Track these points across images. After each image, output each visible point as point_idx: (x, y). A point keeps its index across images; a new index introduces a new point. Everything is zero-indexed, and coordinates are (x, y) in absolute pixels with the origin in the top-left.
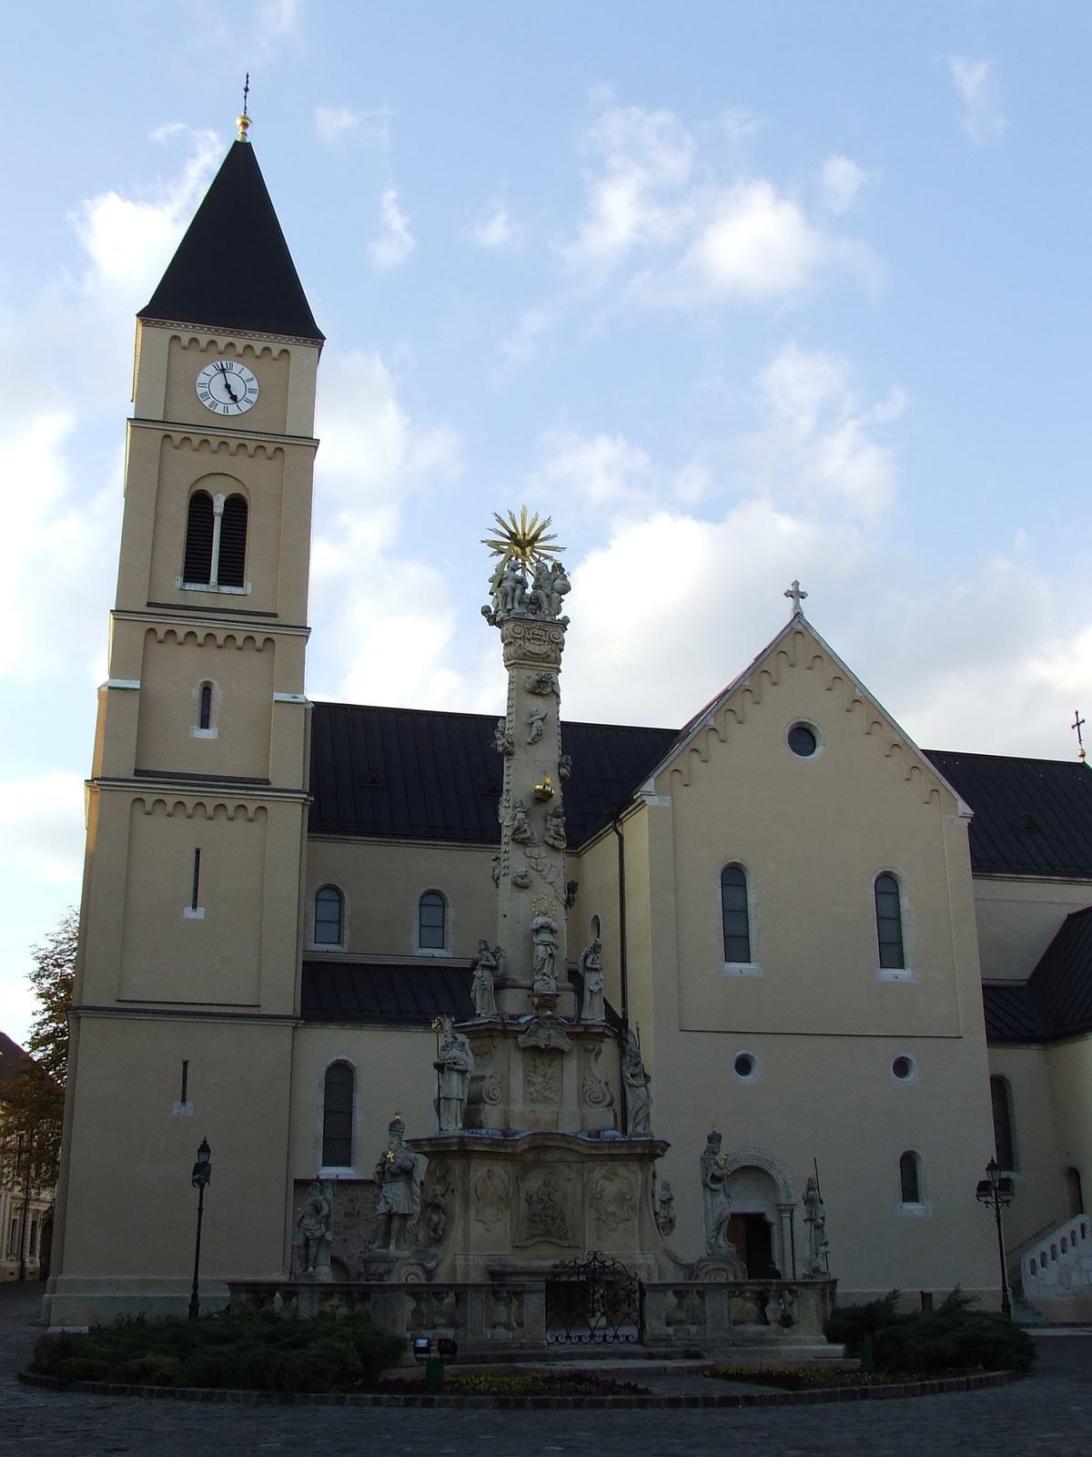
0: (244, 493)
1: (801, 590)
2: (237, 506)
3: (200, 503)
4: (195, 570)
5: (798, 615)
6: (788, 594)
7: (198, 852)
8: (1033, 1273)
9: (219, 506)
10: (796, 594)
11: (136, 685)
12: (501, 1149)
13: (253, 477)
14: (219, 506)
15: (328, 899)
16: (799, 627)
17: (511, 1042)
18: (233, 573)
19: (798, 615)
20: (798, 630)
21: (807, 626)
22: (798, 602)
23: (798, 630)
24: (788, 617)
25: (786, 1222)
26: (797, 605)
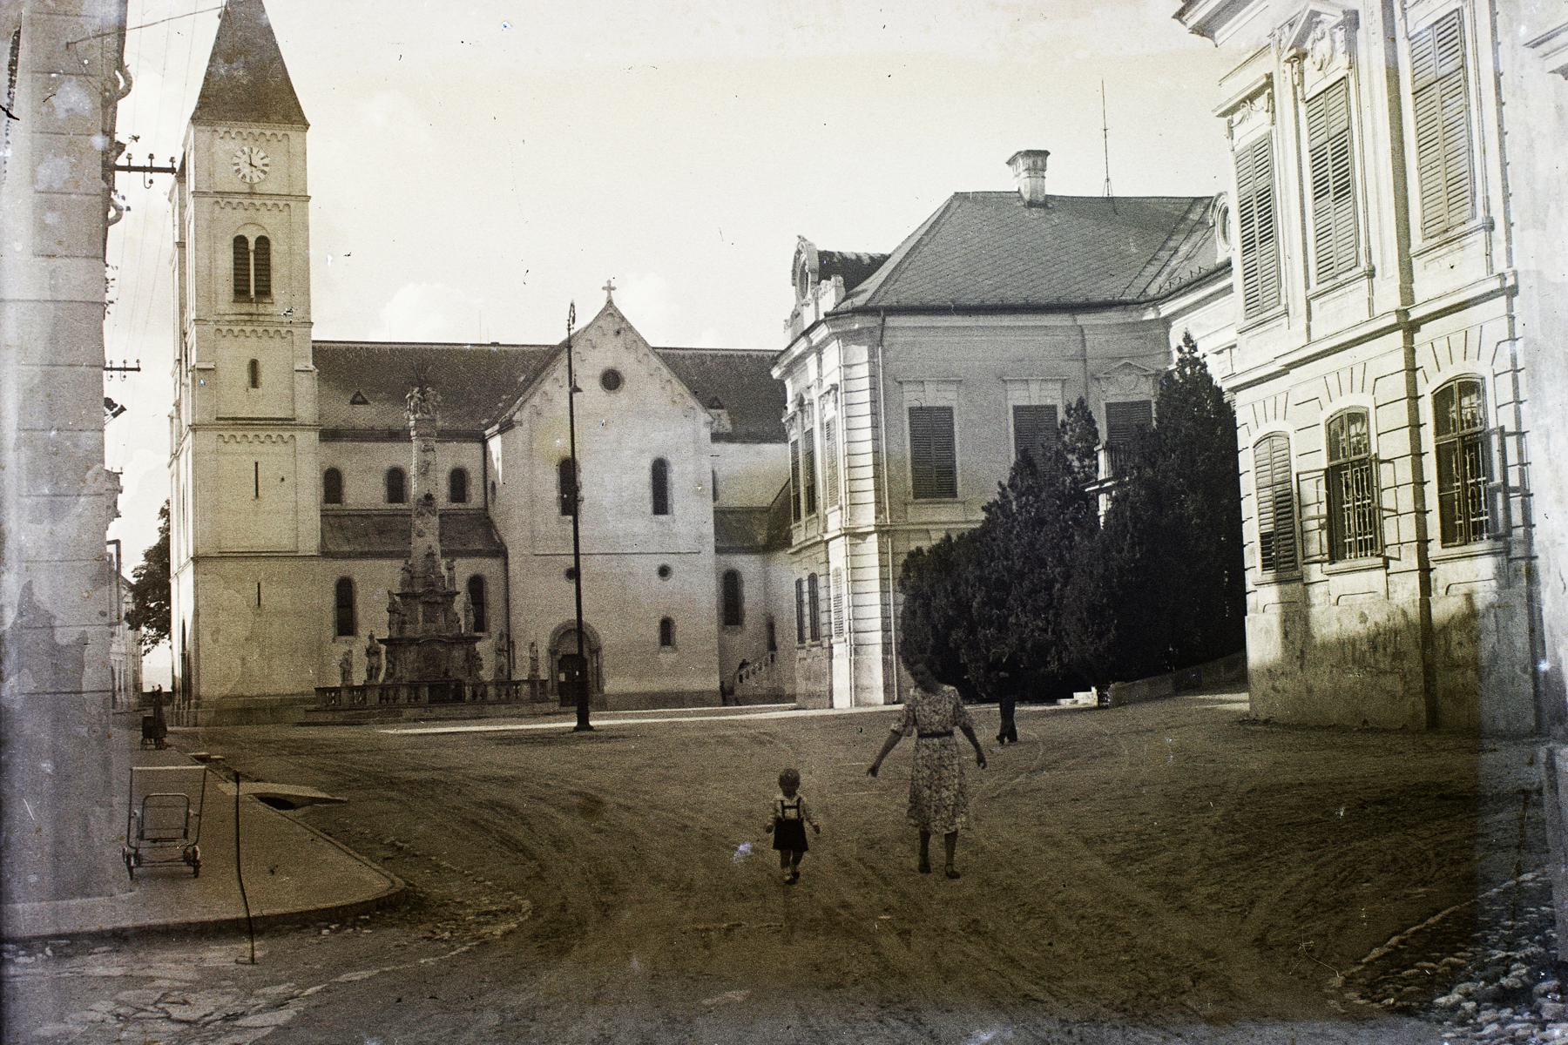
1: (612, 285)
2: (263, 242)
3: (240, 242)
4: (241, 293)
5: (610, 302)
8: (741, 681)
9: (252, 246)
12: (413, 641)
13: (270, 223)
14: (252, 246)
15: (333, 483)
18: (264, 291)
19: (610, 302)
21: (616, 310)
22: (610, 293)
24: (603, 304)
25: (595, 659)
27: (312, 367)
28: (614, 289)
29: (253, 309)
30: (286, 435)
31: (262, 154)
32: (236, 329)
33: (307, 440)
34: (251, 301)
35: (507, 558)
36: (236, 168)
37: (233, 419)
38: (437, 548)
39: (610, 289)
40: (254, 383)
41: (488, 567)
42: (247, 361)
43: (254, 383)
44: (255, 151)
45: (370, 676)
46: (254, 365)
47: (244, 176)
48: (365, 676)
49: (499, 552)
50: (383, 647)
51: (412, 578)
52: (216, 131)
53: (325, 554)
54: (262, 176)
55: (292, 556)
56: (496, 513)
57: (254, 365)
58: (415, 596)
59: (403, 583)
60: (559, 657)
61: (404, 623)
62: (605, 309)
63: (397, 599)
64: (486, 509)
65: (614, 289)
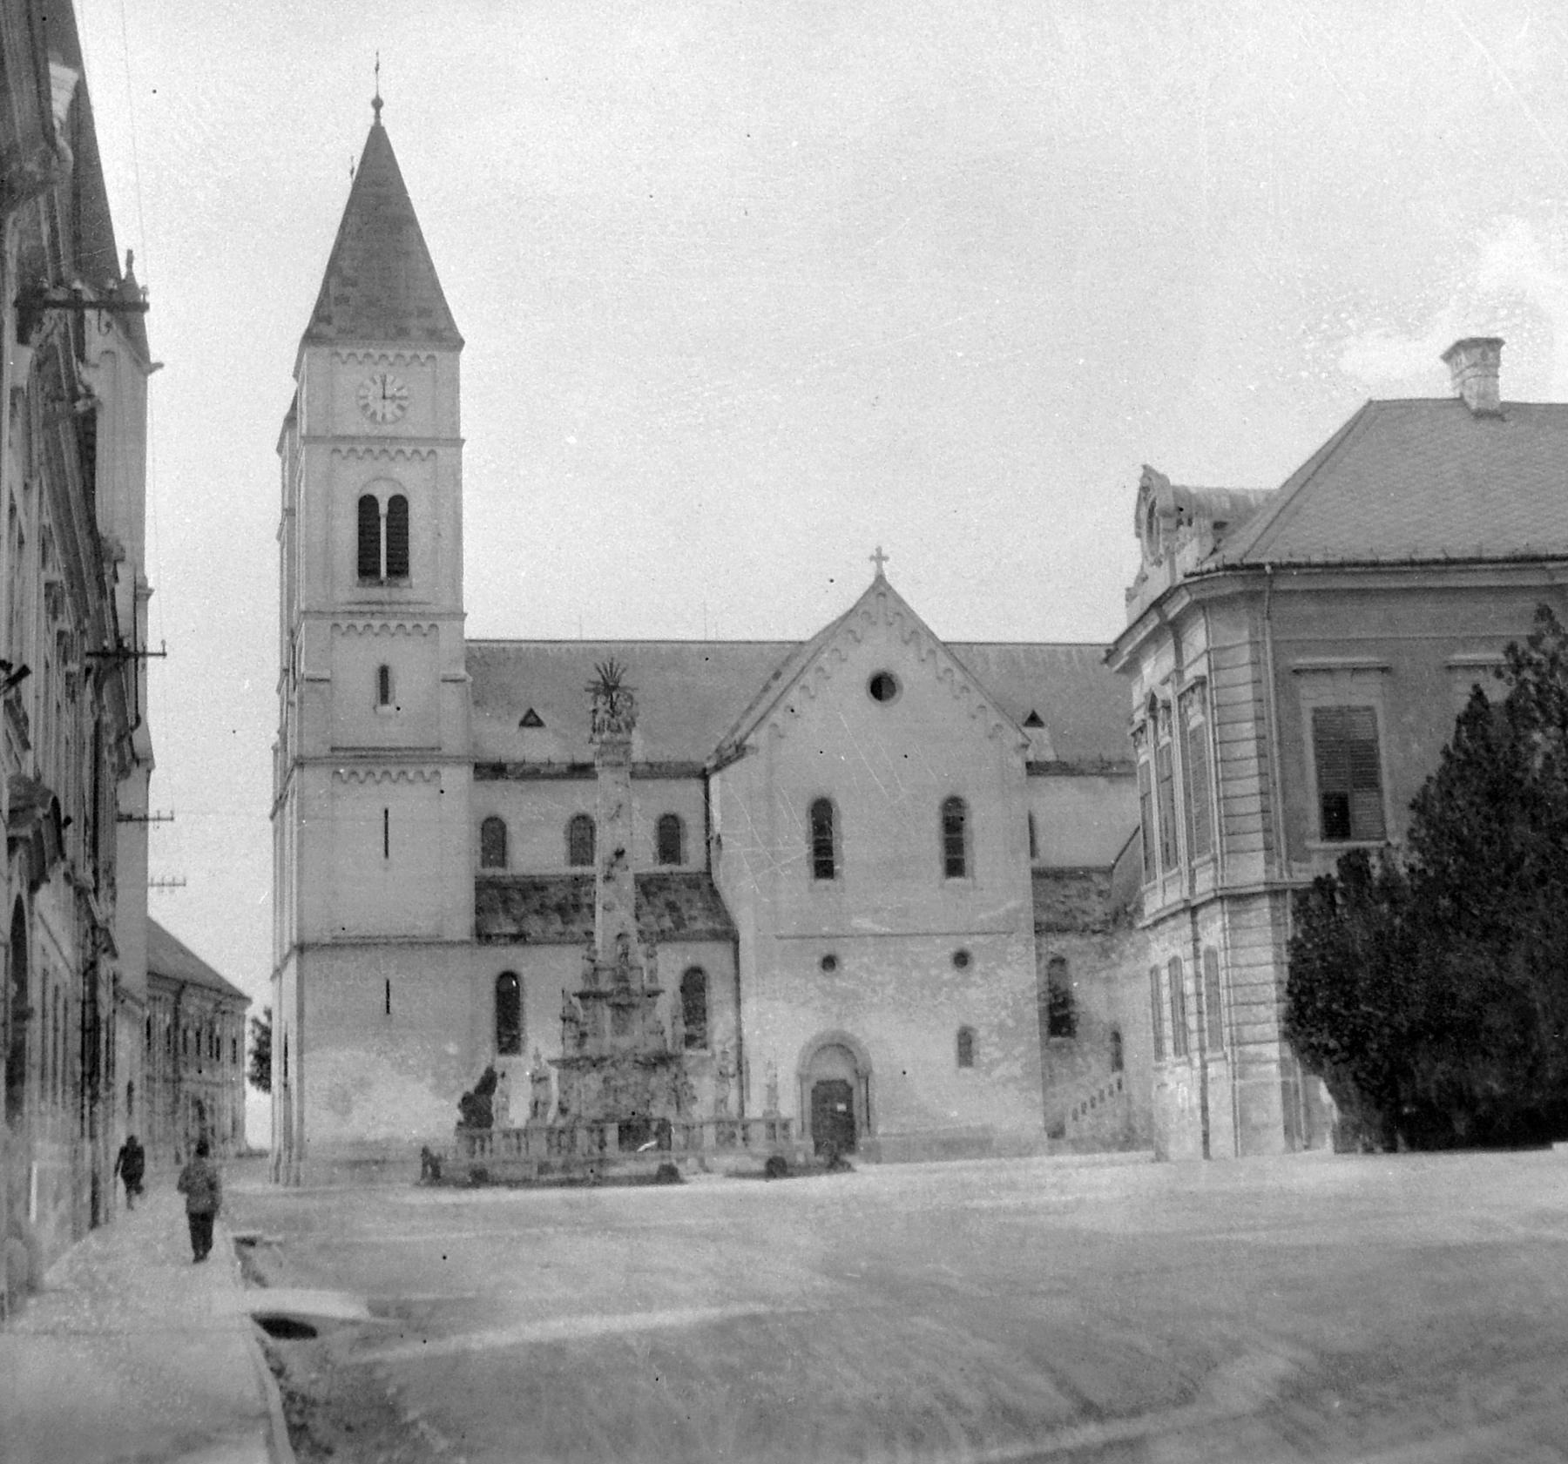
0: (401, 492)
2: (399, 505)
3: (367, 505)
4: (367, 569)
5: (880, 578)
6: (872, 558)
7: (386, 812)
9: (383, 509)
10: (879, 558)
11: (326, 674)
13: (409, 478)
14: (383, 509)
15: (494, 837)
16: (882, 589)
17: (604, 1001)
18: (399, 567)
19: (880, 578)
20: (880, 588)
22: (879, 566)
23: (880, 588)
26: (879, 566)
27: (462, 673)
28: (886, 559)
29: (377, 593)
30: (428, 770)
31: (399, 383)
32: (360, 623)
33: (458, 778)
34: (381, 583)
35: (736, 942)
36: (362, 402)
37: (354, 749)
38: (632, 928)
39: (879, 558)
40: (384, 697)
41: (711, 956)
42: (376, 666)
43: (384, 697)
44: (390, 379)
45: (535, 1114)
46: (384, 672)
47: (374, 414)
48: (527, 1112)
49: (728, 935)
50: (554, 1072)
51: (596, 969)
52: (337, 354)
53: (483, 936)
54: (398, 413)
55: (435, 942)
56: (719, 876)
57: (384, 672)
58: (598, 996)
59: (585, 977)
60: (813, 1083)
61: (583, 1035)
62: (873, 588)
63: (576, 1001)
64: (709, 874)
65: (886, 559)
